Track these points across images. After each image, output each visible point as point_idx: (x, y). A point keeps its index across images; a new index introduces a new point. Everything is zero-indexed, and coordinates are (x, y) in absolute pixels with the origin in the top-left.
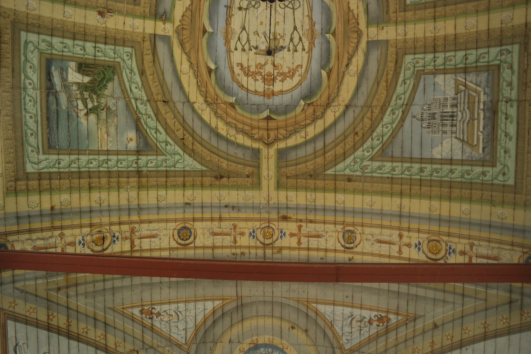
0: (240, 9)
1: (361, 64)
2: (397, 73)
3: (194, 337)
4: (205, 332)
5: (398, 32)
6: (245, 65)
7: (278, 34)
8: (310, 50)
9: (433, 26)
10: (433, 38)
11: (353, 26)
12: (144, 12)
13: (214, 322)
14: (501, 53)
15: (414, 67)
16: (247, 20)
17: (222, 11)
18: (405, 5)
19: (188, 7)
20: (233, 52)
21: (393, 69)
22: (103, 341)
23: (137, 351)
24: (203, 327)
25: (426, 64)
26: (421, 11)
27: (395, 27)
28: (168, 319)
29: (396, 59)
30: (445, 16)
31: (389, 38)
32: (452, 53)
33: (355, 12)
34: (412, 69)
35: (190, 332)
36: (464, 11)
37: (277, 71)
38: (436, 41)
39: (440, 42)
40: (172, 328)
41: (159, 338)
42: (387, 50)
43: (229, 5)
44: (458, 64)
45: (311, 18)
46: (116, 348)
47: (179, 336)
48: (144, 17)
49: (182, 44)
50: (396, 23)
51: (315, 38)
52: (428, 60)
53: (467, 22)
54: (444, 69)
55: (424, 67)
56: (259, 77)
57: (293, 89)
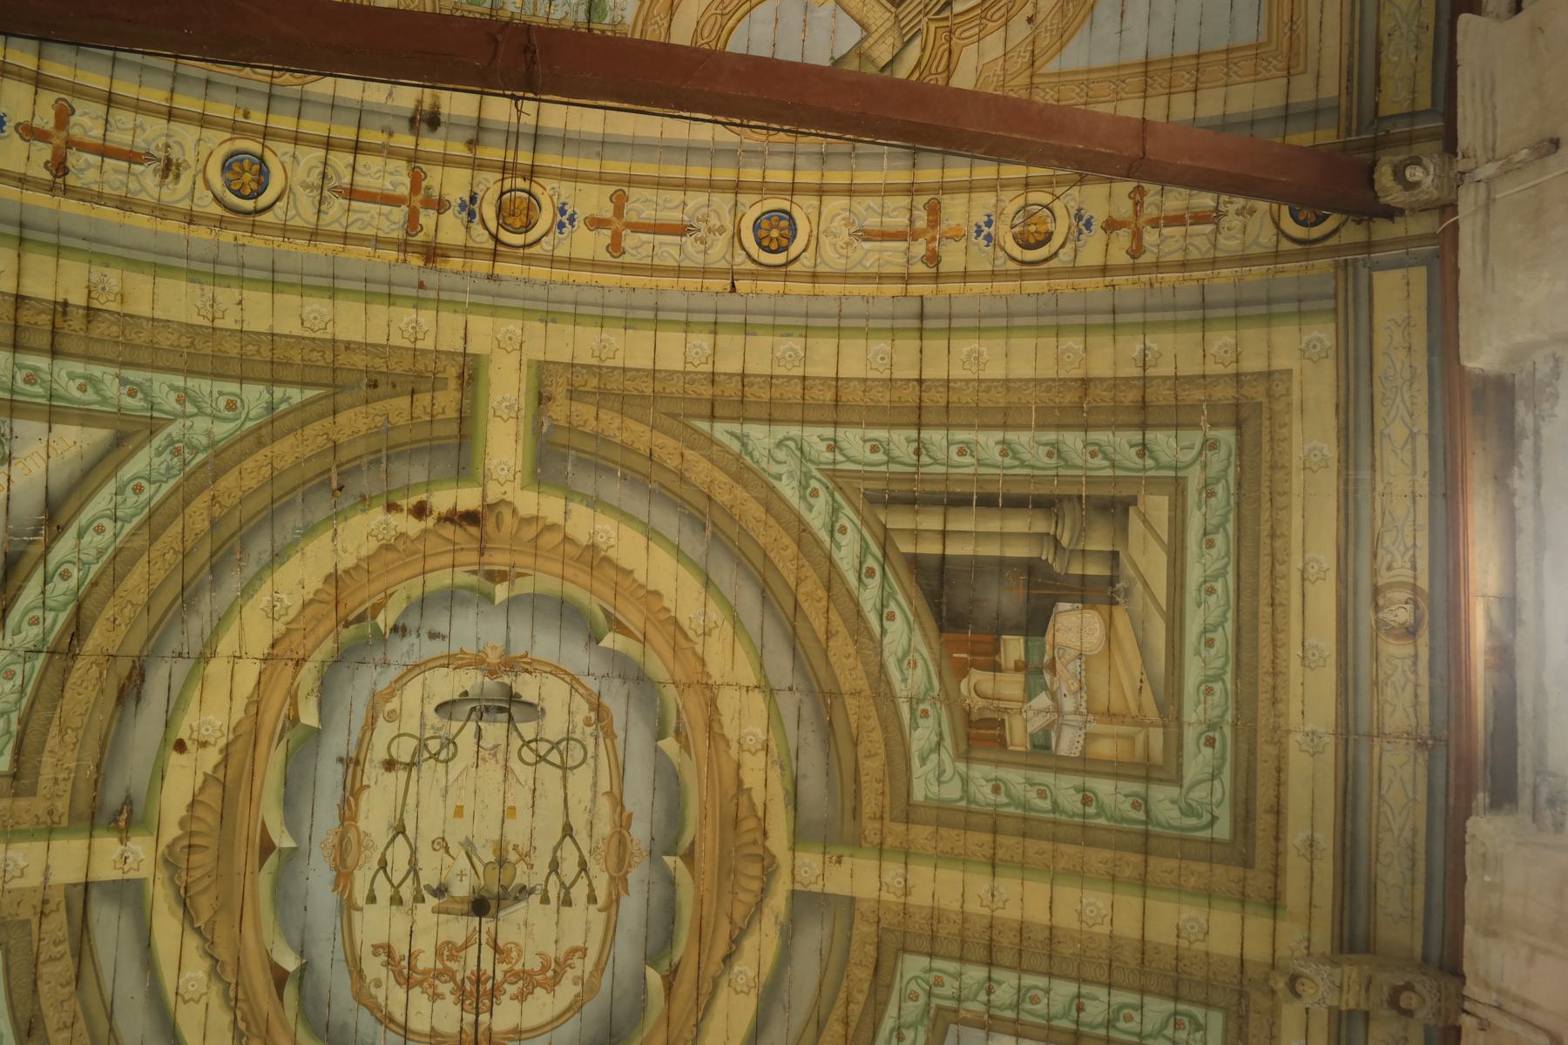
0: (390, 765)
1: (769, 958)
2: (877, 1002)
5: (883, 880)
6: (401, 949)
7: (510, 848)
8: (613, 903)
9: (986, 886)
10: (986, 922)
11: (747, 838)
12: (51, 813)
14: (1175, 1018)
15: (930, 994)
16: (411, 801)
17: (330, 775)
18: (908, 804)
19: (210, 772)
20: (361, 909)
21: (866, 986)
25: (965, 993)
26: (953, 833)
27: (877, 863)
29: (877, 960)
30: (1023, 867)
31: (858, 894)
32: (1042, 982)
33: (758, 796)
34: (922, 1000)
36: (1078, 868)
37: (505, 967)
38: (995, 932)
39: (1007, 940)
42: (851, 928)
43: (353, 754)
44: (1056, 1017)
45: (618, 803)
48: (49, 830)
49: (185, 903)
50: (881, 850)
51: (630, 866)
52: (971, 982)
53: (1084, 901)
54: (1017, 1021)
55: (959, 1000)
56: (445, 988)
57: (555, 1024)
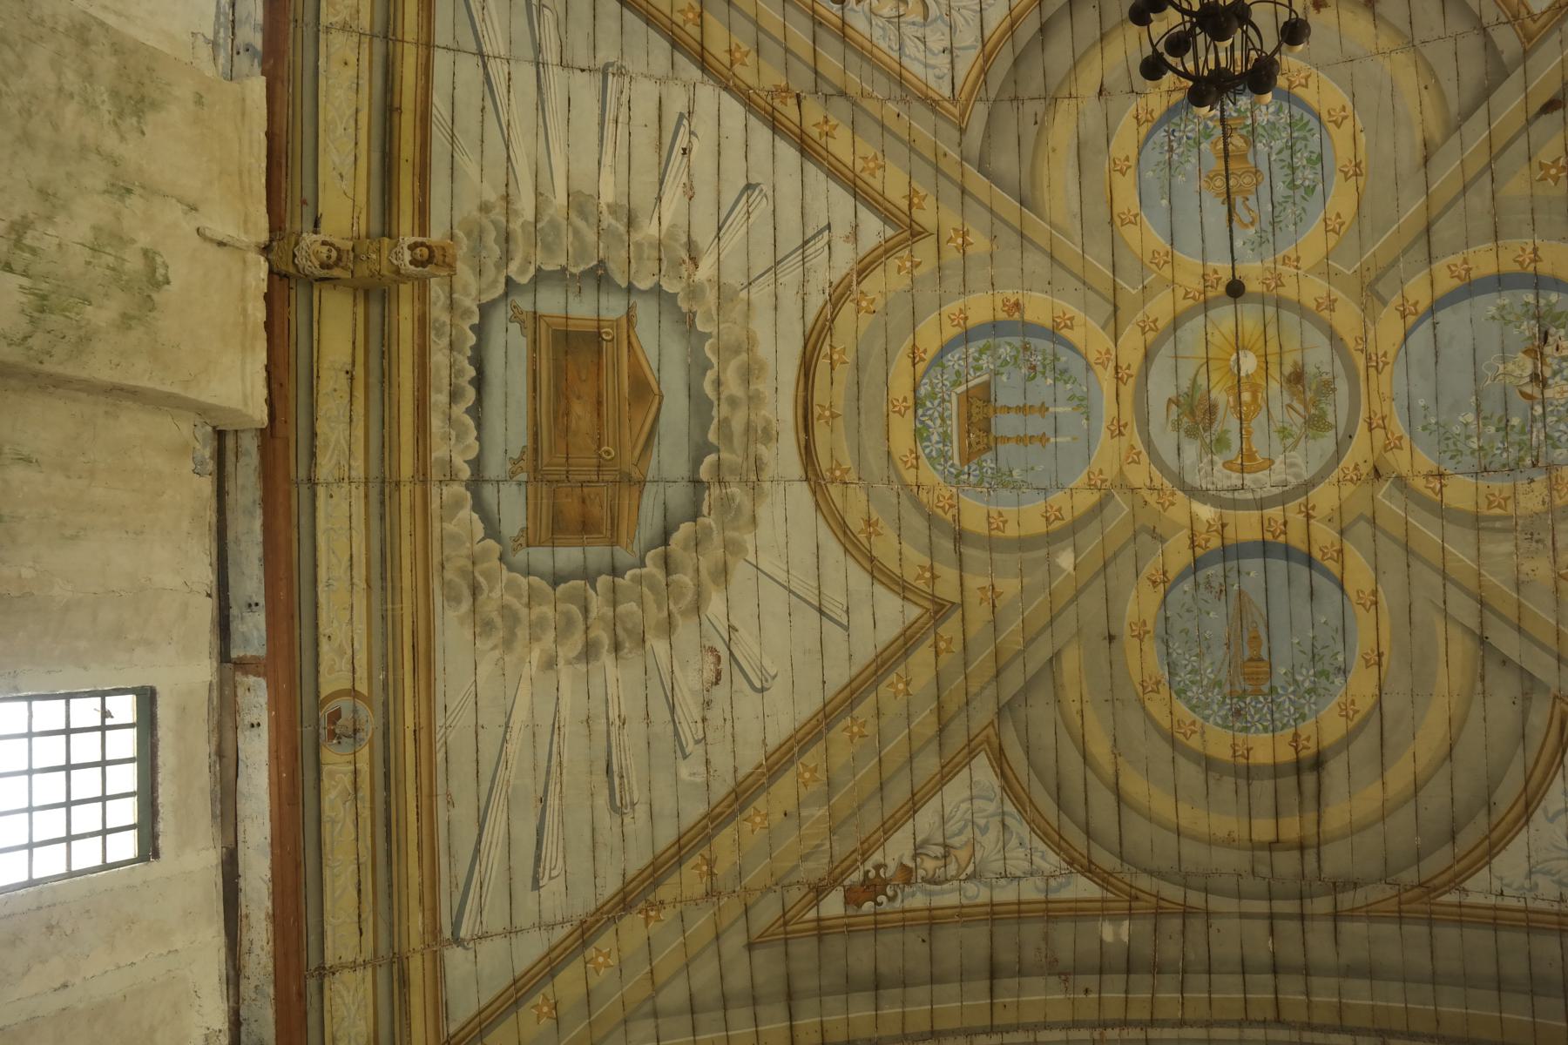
3: (978, 77)
4: (1016, 63)
13: (1043, 29)
22: (694, 30)
23: (798, 96)
24: (1009, 43)
28: (894, 13)
35: (968, 61)
40: (907, 42)
41: (865, 65)
46: (732, 65)
47: (930, 72)
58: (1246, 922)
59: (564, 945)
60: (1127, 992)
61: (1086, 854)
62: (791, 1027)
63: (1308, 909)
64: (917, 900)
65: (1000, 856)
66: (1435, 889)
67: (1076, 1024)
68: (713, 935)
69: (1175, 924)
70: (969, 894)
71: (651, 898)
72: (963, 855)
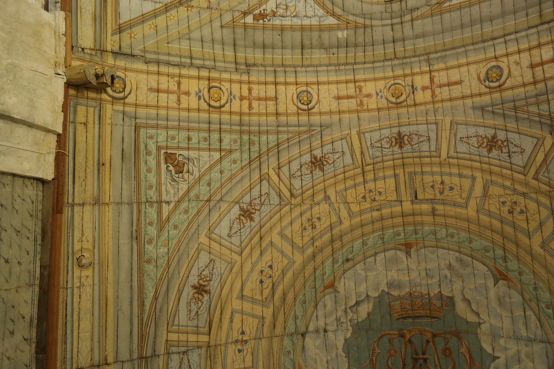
58: (384, 27)
59: (161, 9)
60: (346, 54)
61: (332, 10)
62: (235, 55)
63: (403, 20)
64: (277, 22)
65: (304, 10)
66: (442, 3)
67: (330, 65)
68: (210, 20)
69: (361, 31)
70: (294, 21)
71: (189, 3)
72: (292, 9)
